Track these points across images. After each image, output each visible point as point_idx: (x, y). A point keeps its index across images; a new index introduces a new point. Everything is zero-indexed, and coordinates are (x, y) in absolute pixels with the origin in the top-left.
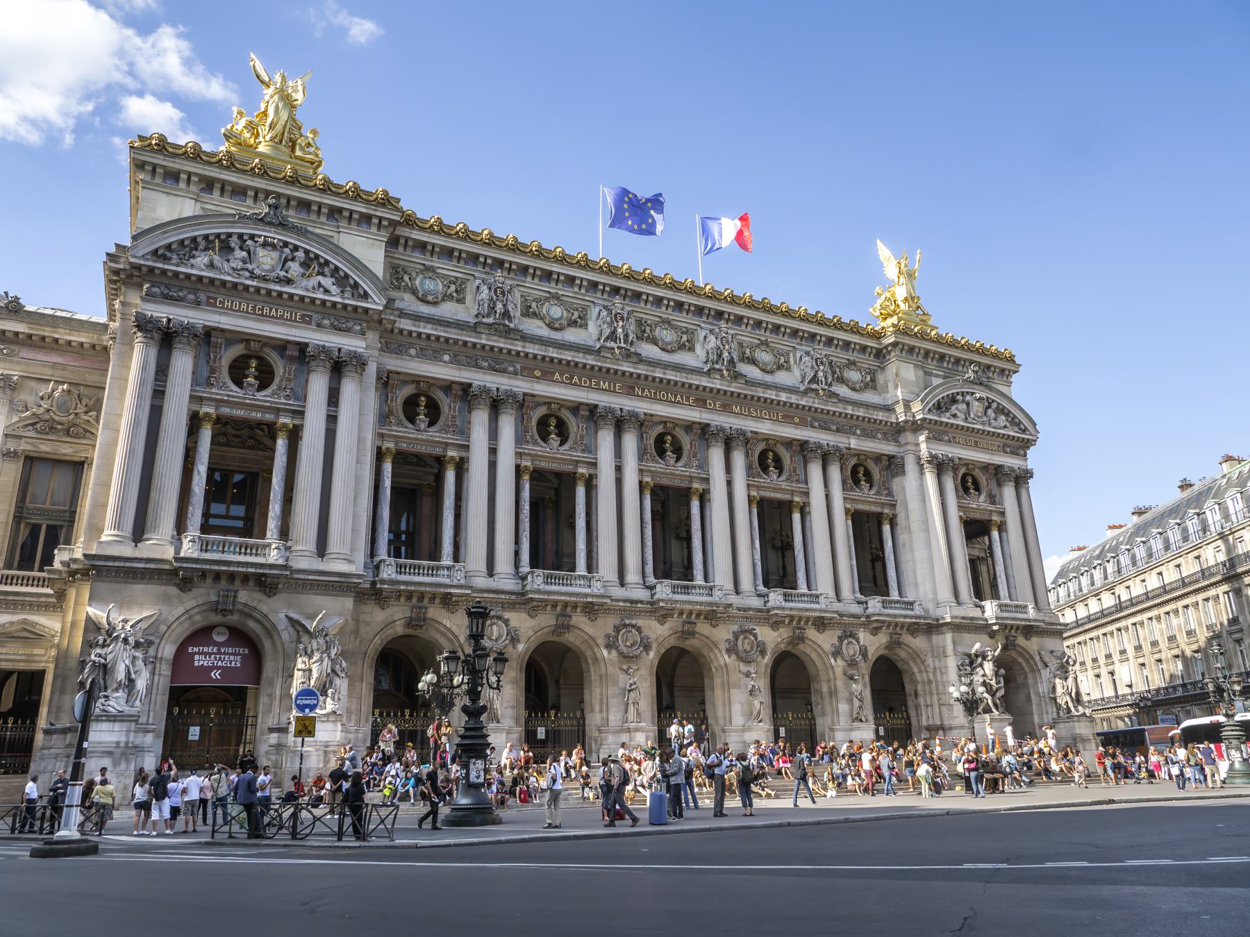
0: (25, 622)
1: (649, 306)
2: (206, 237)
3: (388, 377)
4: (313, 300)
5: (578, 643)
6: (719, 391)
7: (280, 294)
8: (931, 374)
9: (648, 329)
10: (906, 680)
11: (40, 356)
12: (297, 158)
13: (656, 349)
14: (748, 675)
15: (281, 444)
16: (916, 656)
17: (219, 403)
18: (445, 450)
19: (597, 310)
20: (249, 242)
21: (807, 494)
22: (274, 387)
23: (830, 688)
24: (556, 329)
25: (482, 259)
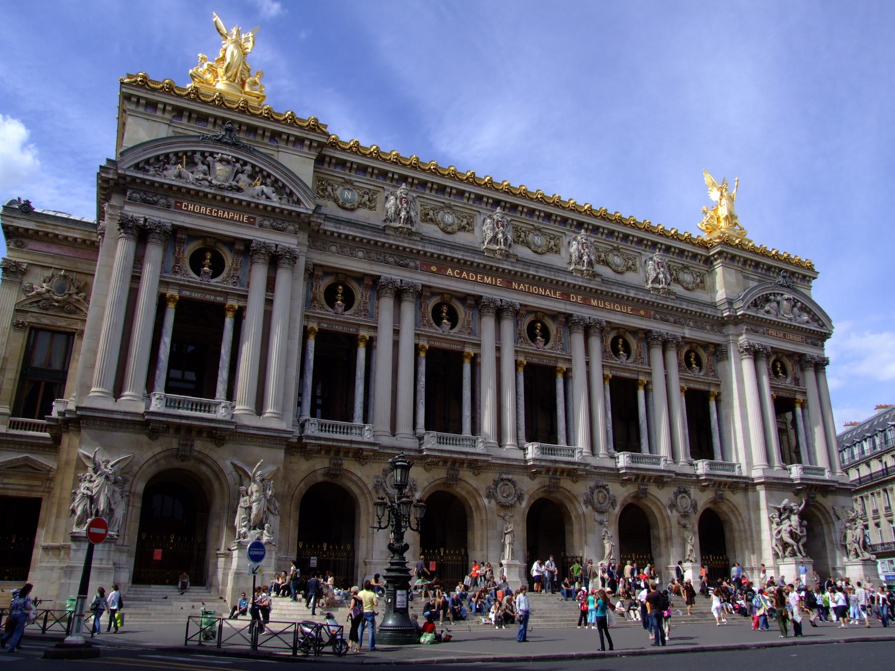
0: (26, 458)
1: (523, 216)
2: (176, 154)
3: (313, 269)
4: (257, 205)
5: (463, 493)
6: (580, 287)
7: (232, 200)
9: (523, 235)
10: (726, 530)
11: (42, 247)
12: (245, 93)
13: (529, 251)
14: (601, 523)
15: (229, 322)
16: (734, 509)
17: (182, 287)
18: (358, 330)
19: (482, 218)
20: (209, 159)
21: (649, 374)
22: (224, 275)
23: (666, 534)
25: (390, 175)
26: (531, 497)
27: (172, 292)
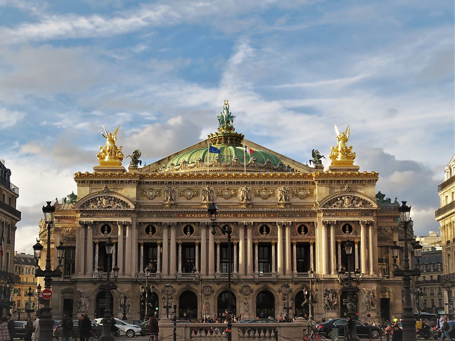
8: (334, 188)
24: (189, 199)
26: (218, 291)
27: (97, 241)
